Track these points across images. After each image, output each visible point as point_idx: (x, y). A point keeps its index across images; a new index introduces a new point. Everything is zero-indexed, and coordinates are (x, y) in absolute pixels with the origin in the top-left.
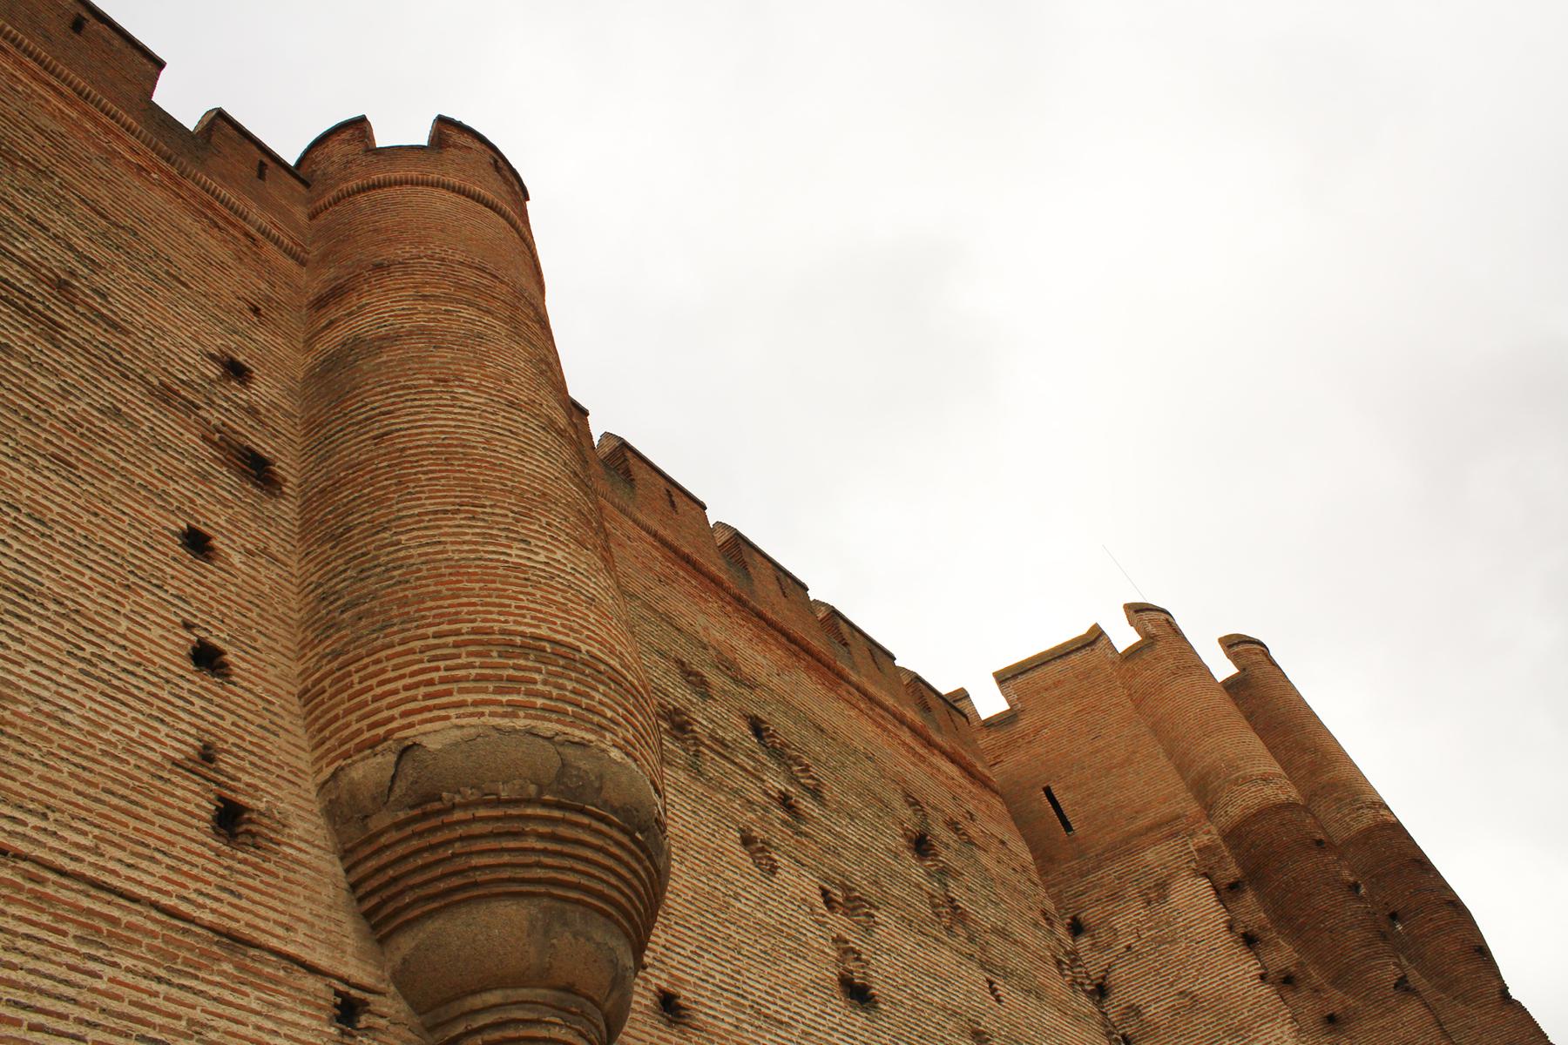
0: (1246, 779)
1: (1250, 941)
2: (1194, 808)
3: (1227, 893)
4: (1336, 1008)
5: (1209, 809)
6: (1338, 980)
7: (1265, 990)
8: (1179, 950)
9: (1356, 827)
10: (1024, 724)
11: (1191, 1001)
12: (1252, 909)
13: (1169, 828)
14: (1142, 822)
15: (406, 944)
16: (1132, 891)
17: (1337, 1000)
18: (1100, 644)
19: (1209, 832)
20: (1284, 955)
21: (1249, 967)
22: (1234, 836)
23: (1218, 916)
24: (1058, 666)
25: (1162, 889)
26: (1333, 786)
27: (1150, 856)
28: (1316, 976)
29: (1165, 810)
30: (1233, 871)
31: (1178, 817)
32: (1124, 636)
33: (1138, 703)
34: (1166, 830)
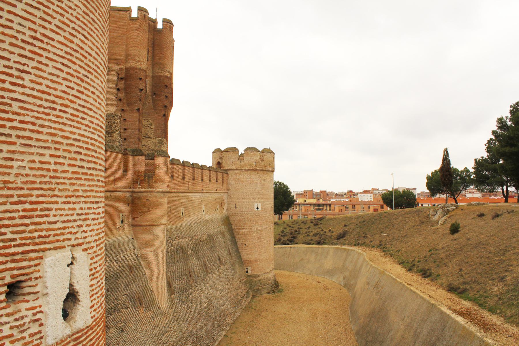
1: (118, 90)
2: (124, 60)
3: (120, 79)
4: (125, 108)
5: (126, 62)
6: (128, 104)
7: (115, 100)
9: (160, 74)
12: (122, 84)
18: (128, 13)
19: (124, 66)
20: (122, 95)
21: (115, 95)
22: (127, 69)
23: (115, 82)
24: (116, 12)
26: (161, 64)
28: (125, 101)
29: (119, 57)
30: (123, 76)
31: (120, 60)
32: (135, 14)
34: (116, 61)
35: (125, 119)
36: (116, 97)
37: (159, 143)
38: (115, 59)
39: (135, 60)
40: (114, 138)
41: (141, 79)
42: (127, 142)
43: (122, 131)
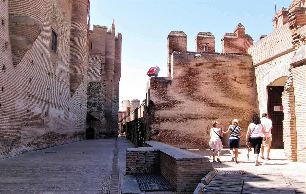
1: (102, 70)
2: (104, 54)
5: (106, 55)
6: (107, 77)
7: (100, 75)
8: (95, 67)
10: (94, 33)
11: (94, 72)
12: (103, 68)
14: (99, 52)
15: (71, 84)
17: (106, 79)
20: (104, 73)
24: (100, 29)
29: (102, 52)
30: (104, 62)
33: (106, 39)
34: (101, 55)
35: (105, 85)
36: (101, 73)
37: (116, 97)
40: (100, 95)
41: (113, 65)
43: (104, 91)
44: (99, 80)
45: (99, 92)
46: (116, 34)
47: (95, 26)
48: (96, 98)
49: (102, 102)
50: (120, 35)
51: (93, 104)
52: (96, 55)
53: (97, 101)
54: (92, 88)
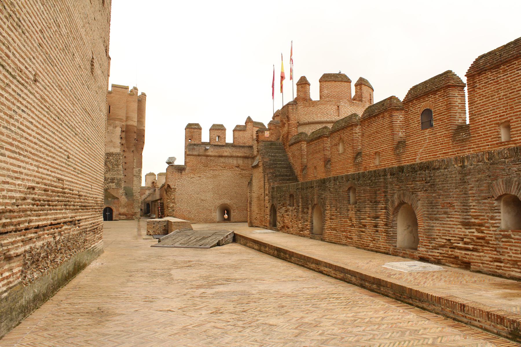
0: (133, 121)
1: (121, 138)
2: (125, 119)
3: (122, 131)
4: (125, 150)
5: (126, 121)
6: (127, 148)
7: (120, 144)
8: (113, 135)
10: (112, 95)
12: (124, 135)
13: (121, 120)
14: (118, 117)
16: (112, 125)
20: (124, 142)
22: (127, 126)
23: (120, 134)
24: (120, 89)
25: (116, 127)
27: (117, 122)
28: (125, 146)
29: (122, 118)
30: (124, 129)
33: (127, 102)
38: (119, 119)
39: (133, 121)
40: (120, 168)
42: (126, 171)
43: (124, 164)
44: (117, 150)
45: (118, 165)
46: (139, 94)
47: (113, 86)
48: (114, 172)
49: (122, 177)
50: (144, 95)
51: (110, 179)
52: (115, 120)
53: (114, 176)
54: (109, 160)
